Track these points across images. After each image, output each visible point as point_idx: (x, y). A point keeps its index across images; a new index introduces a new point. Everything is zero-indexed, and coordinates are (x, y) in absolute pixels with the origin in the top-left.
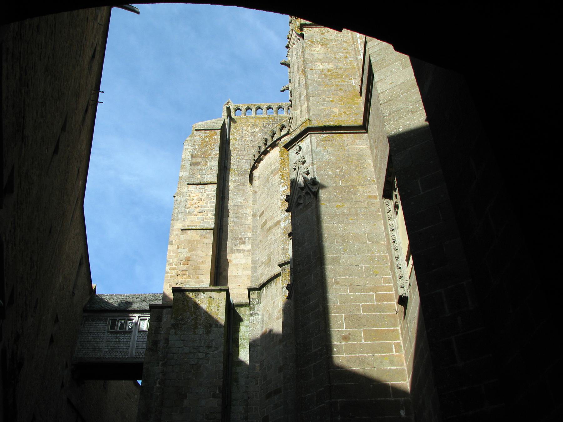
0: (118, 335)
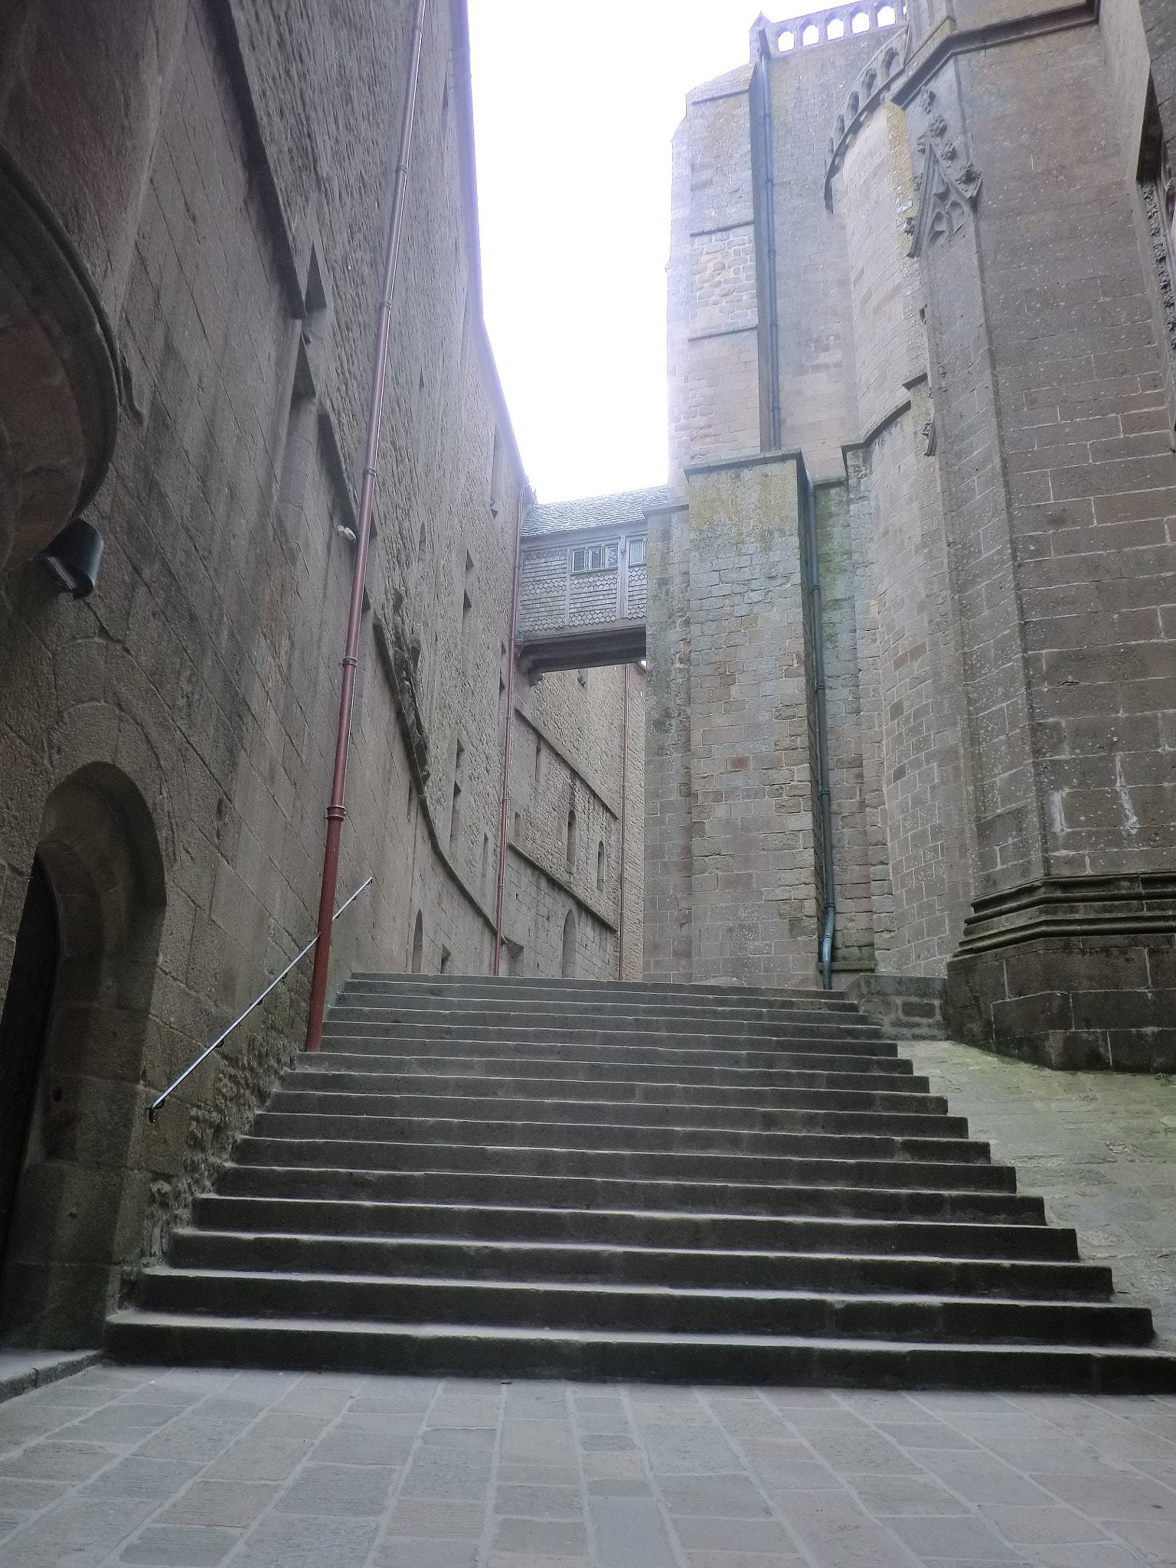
0: (591, 579)
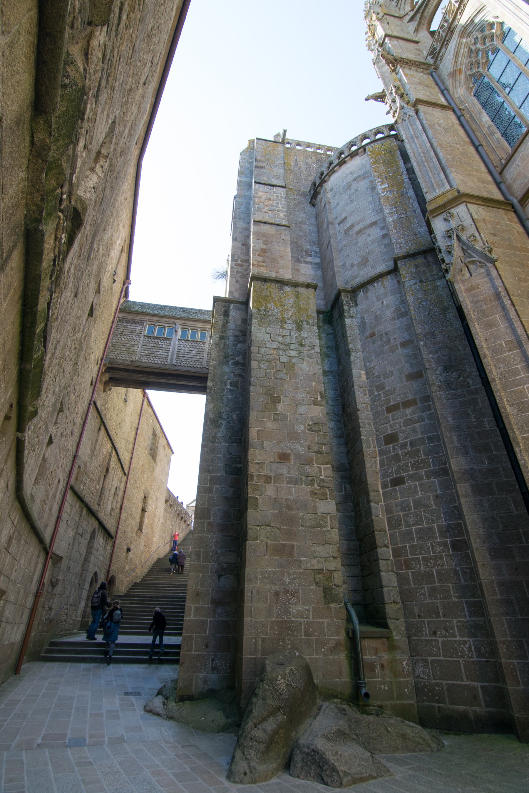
0: (156, 341)
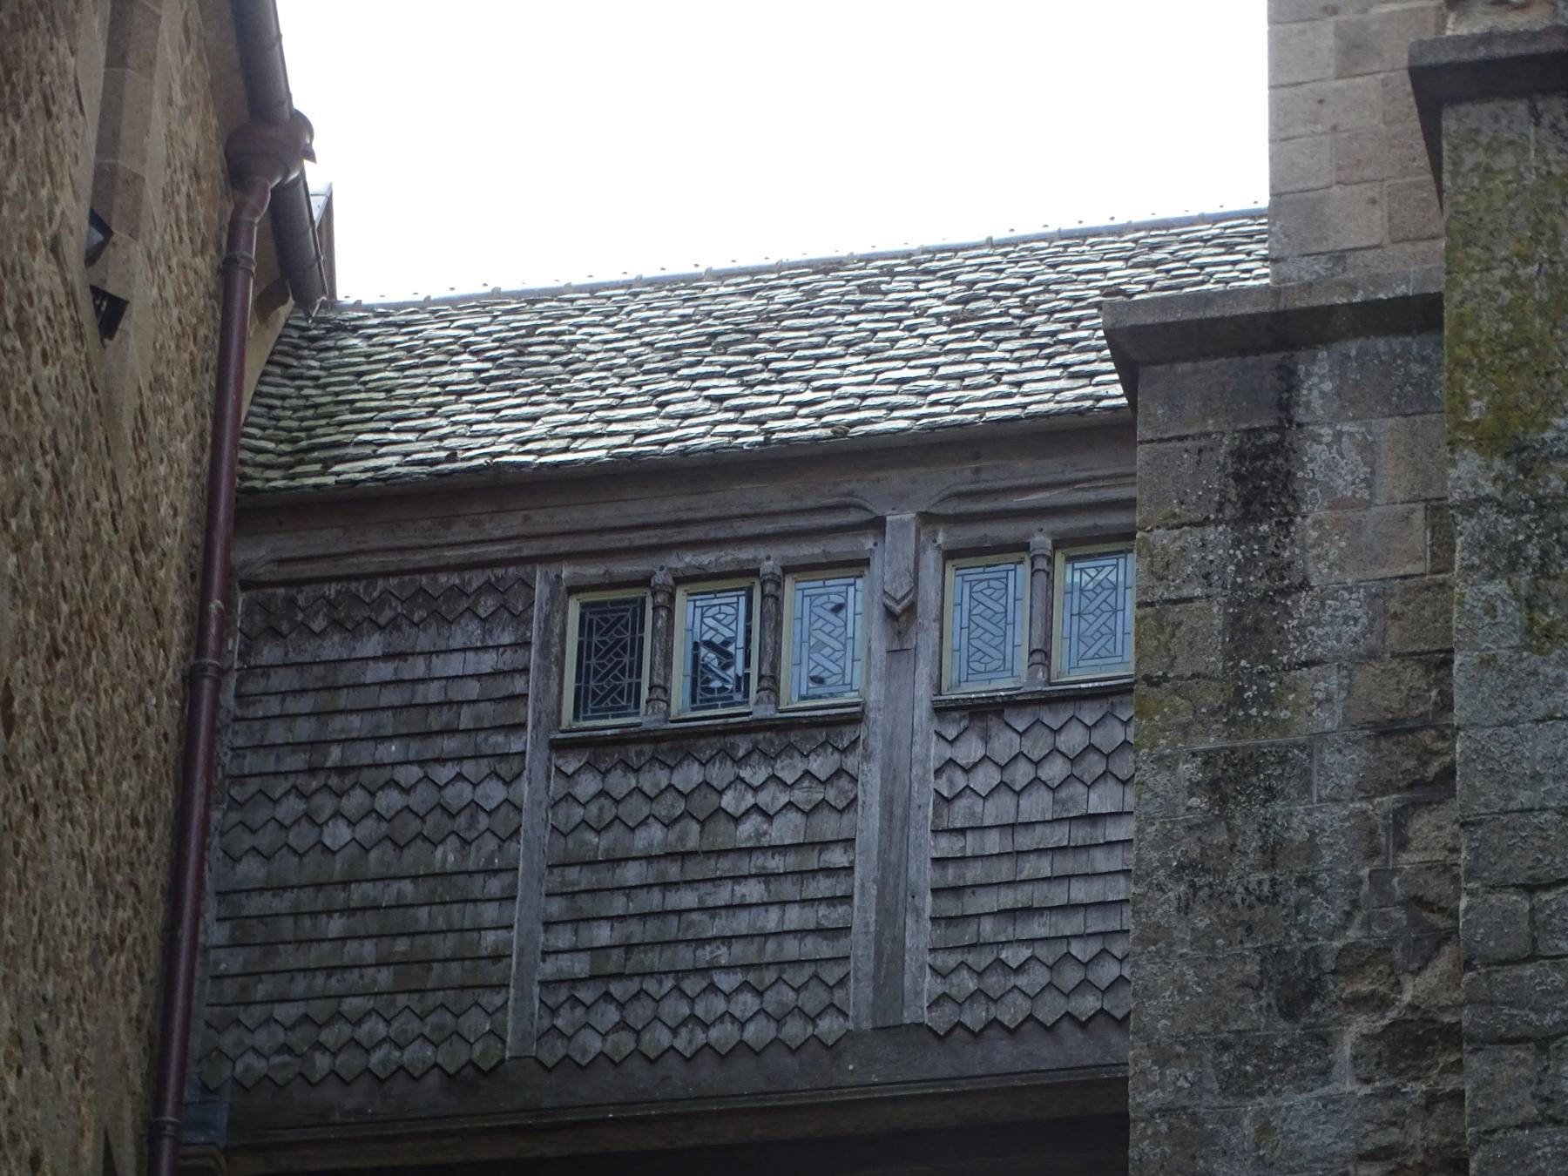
0: (689, 775)
